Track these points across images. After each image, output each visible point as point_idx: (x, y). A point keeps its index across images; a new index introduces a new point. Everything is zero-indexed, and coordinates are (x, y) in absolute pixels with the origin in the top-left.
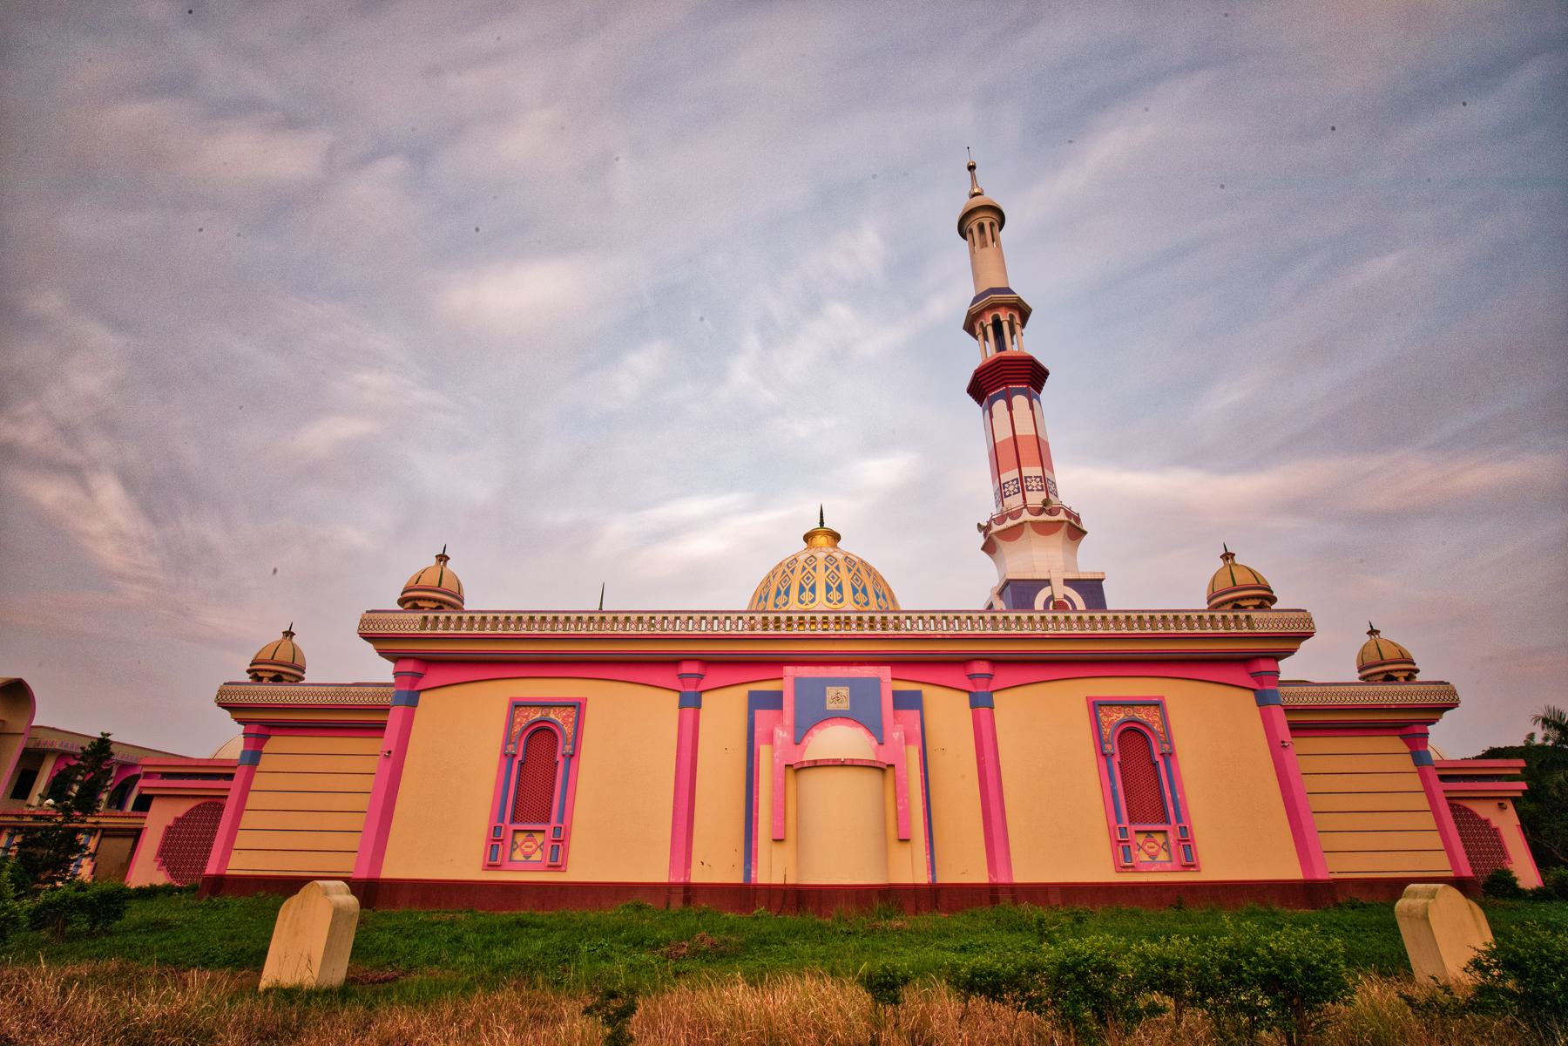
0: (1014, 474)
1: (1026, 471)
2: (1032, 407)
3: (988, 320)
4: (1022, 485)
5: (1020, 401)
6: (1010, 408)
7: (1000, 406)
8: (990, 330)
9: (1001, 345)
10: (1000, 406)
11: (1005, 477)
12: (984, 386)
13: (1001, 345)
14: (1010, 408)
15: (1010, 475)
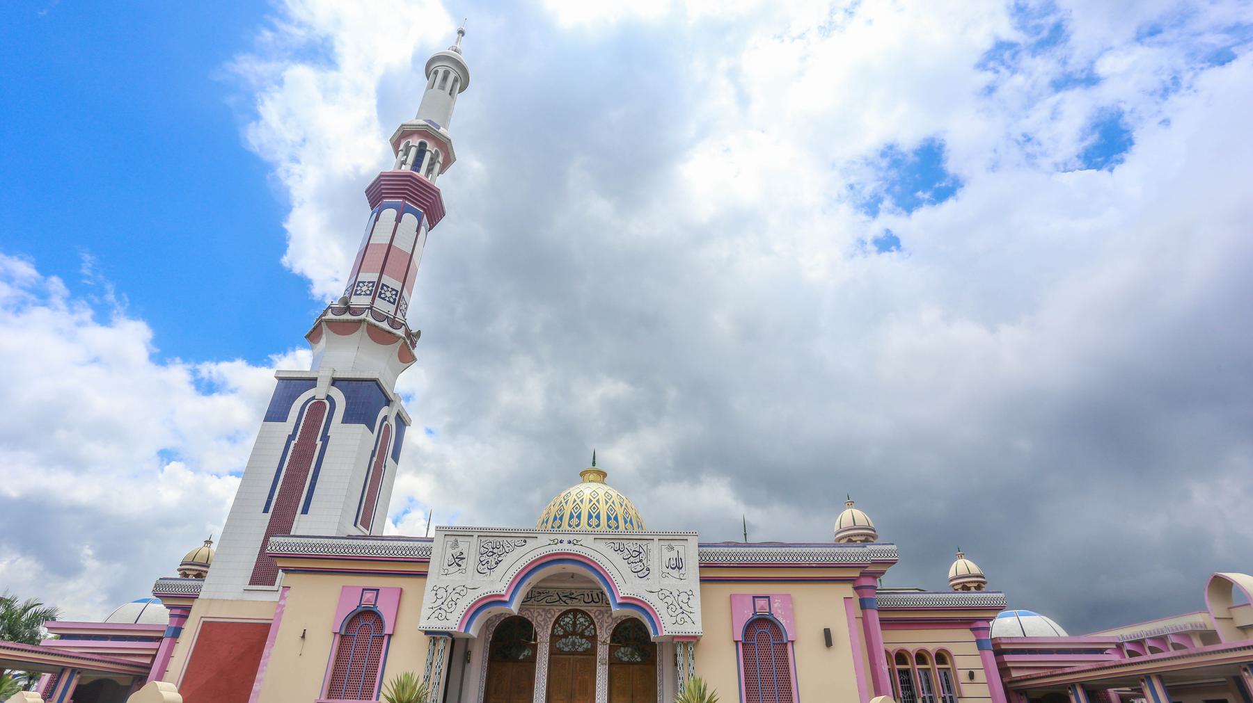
0: (374, 277)
1: (386, 280)
2: (418, 230)
3: (415, 141)
4: (377, 290)
5: (409, 220)
6: (398, 219)
7: (389, 215)
8: (413, 152)
9: (417, 165)
10: (389, 215)
11: (363, 277)
12: (381, 192)
13: (417, 165)
14: (398, 219)
15: (369, 276)
